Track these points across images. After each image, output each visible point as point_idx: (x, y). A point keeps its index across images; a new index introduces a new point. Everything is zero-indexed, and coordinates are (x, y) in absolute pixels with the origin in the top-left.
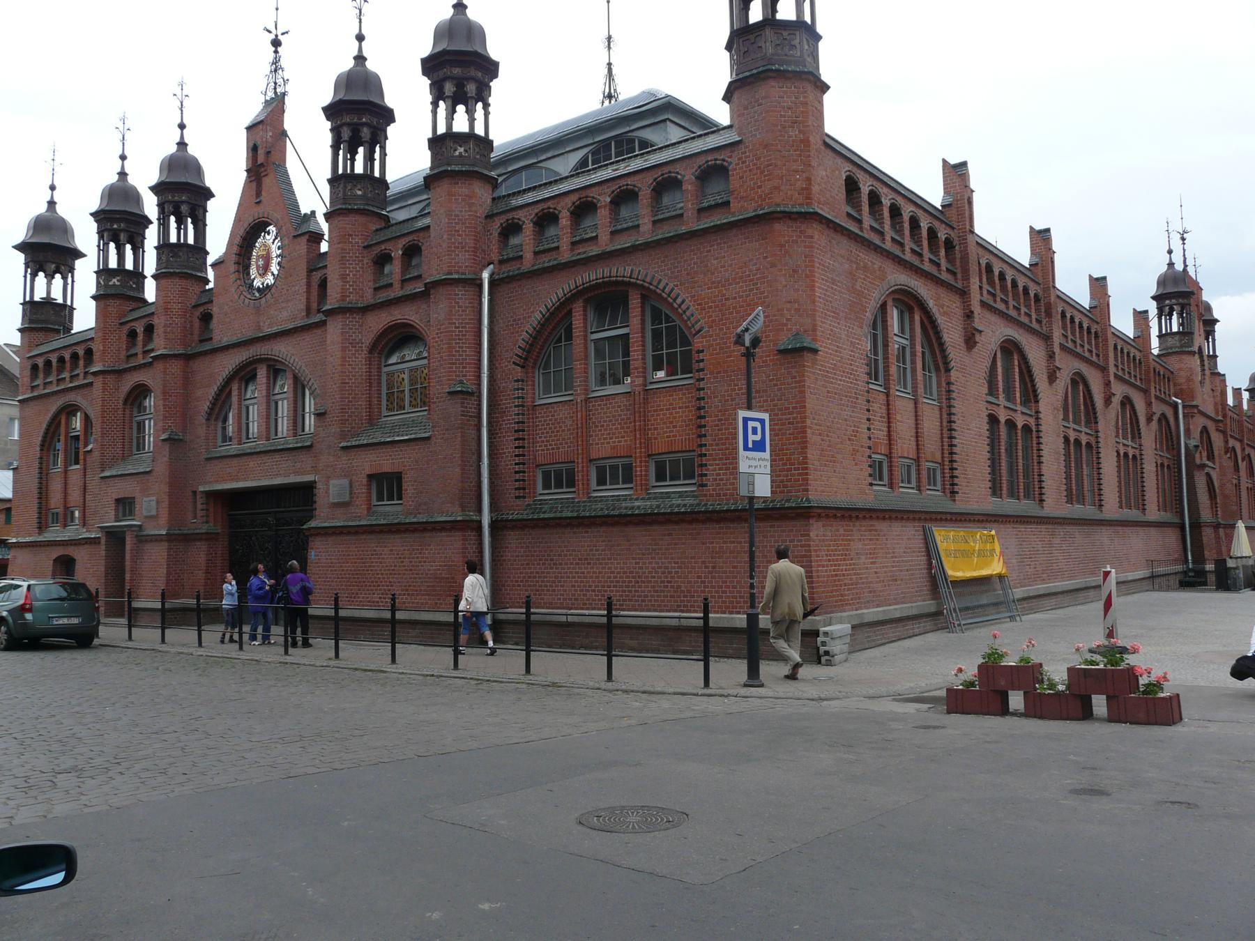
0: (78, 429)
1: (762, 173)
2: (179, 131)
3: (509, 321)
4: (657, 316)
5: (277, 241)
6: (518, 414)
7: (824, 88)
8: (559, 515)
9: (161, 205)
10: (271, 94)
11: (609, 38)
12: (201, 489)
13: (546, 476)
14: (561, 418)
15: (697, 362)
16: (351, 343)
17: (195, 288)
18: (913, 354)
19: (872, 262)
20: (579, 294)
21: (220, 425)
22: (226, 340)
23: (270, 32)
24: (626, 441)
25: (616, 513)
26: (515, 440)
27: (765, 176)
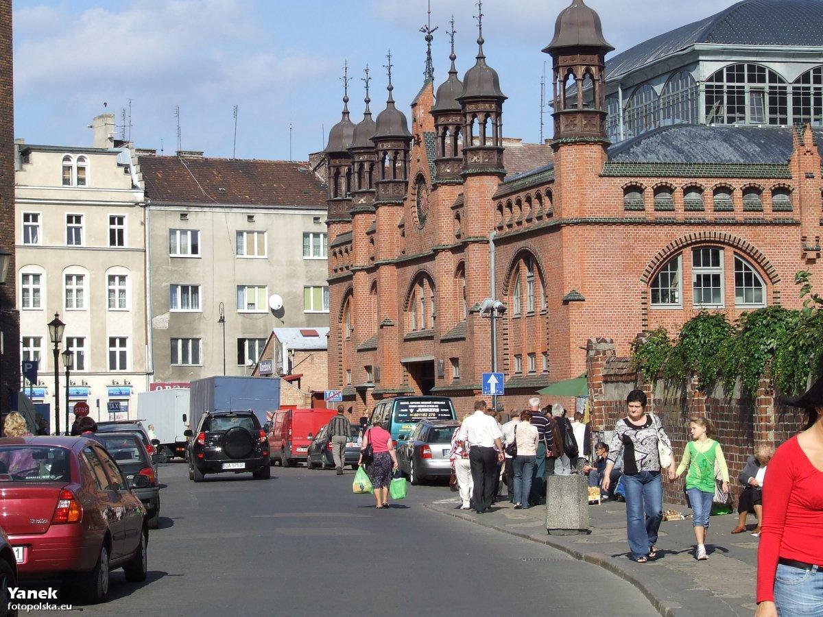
16: (445, 272)
23: (425, 31)
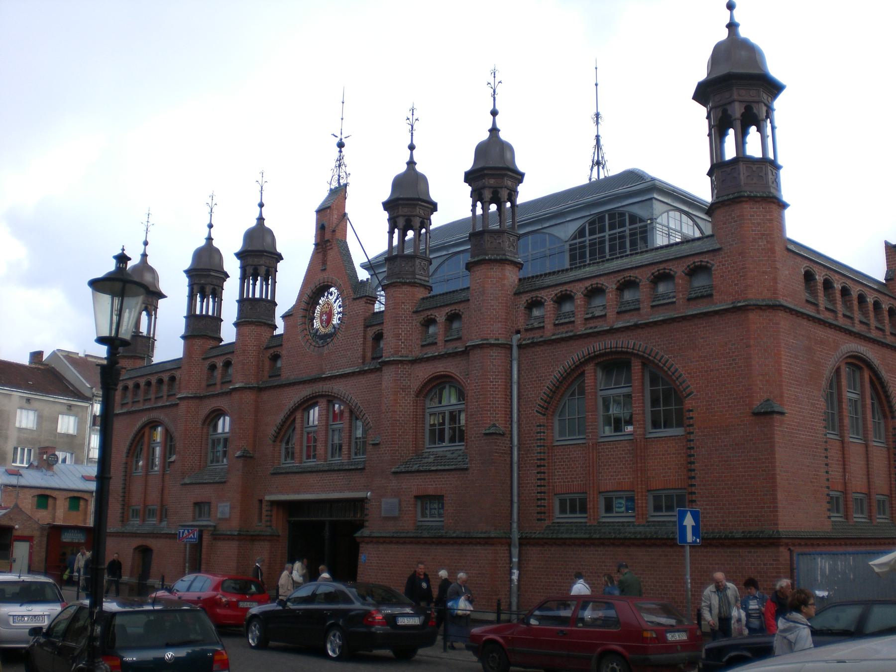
0: (158, 440)
1: (738, 273)
2: (259, 209)
3: (533, 378)
4: (654, 381)
5: (338, 301)
6: (540, 453)
7: (784, 206)
8: (573, 536)
9: (243, 268)
10: (335, 185)
11: (597, 115)
12: (267, 498)
13: (563, 502)
14: (575, 457)
15: (688, 418)
16: (402, 389)
17: (264, 332)
18: (864, 406)
19: (827, 336)
20: (591, 359)
21: (284, 445)
22: (293, 378)
23: (336, 137)
24: (629, 478)
25: (622, 536)
26: (538, 473)
27: (741, 276)
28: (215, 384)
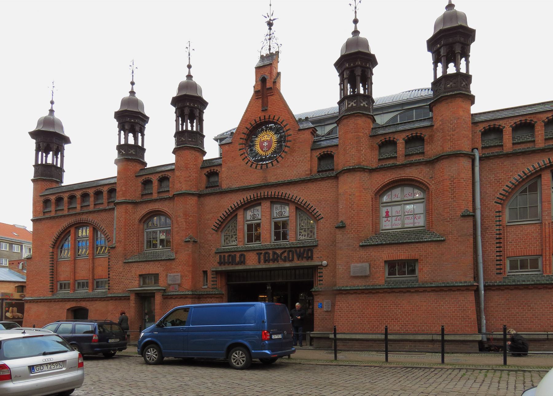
28: (152, 193)
